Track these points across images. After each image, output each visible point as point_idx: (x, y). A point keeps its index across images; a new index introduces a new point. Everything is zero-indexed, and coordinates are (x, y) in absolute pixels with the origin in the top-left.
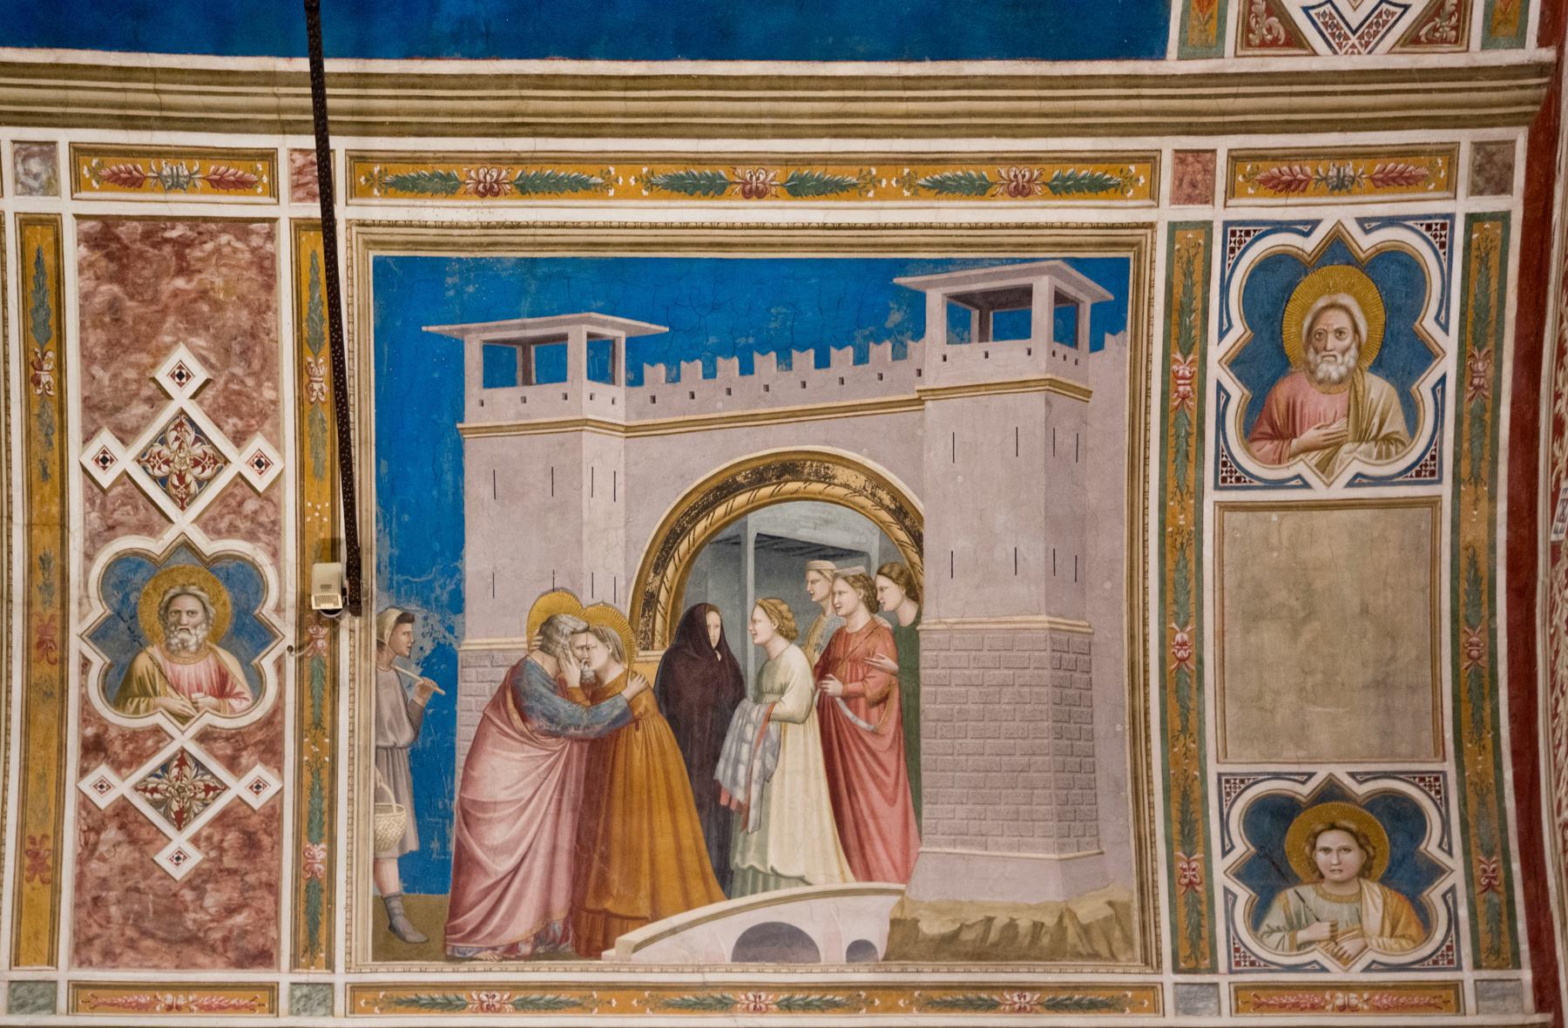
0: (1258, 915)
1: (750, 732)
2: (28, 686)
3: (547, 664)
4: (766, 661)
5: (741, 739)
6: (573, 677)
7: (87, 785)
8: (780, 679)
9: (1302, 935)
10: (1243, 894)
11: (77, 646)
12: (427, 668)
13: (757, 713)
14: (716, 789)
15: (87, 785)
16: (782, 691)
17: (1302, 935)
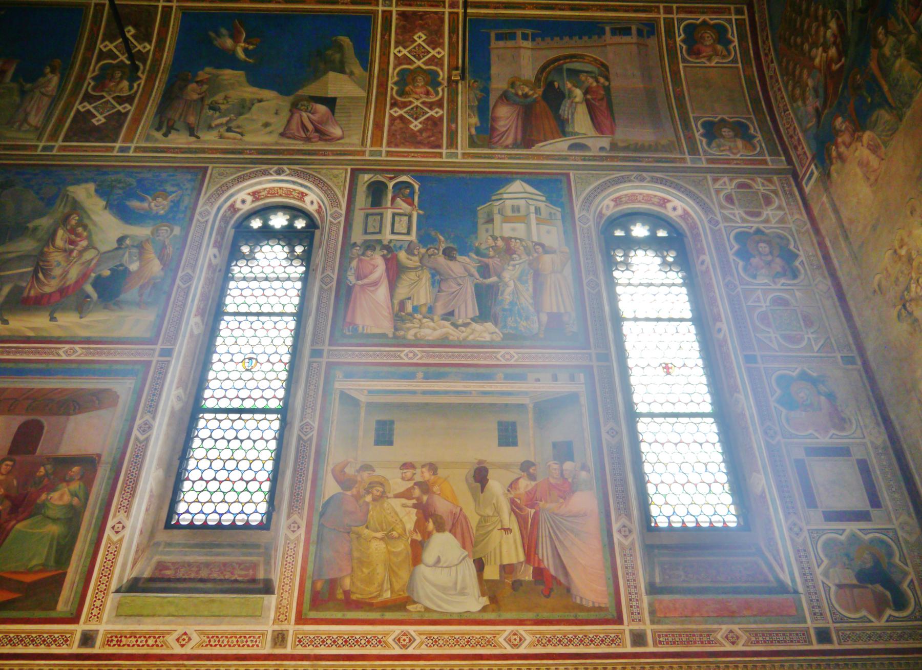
0: (709, 144)
1: (567, 105)
2: (377, 92)
3: (513, 91)
4: (570, 91)
5: (565, 106)
6: (520, 93)
7: (392, 112)
8: (574, 95)
9: (722, 149)
10: (704, 140)
11: (390, 85)
12: (481, 91)
13: (569, 101)
14: (560, 116)
15: (392, 112)
16: (575, 97)
17: (722, 149)
